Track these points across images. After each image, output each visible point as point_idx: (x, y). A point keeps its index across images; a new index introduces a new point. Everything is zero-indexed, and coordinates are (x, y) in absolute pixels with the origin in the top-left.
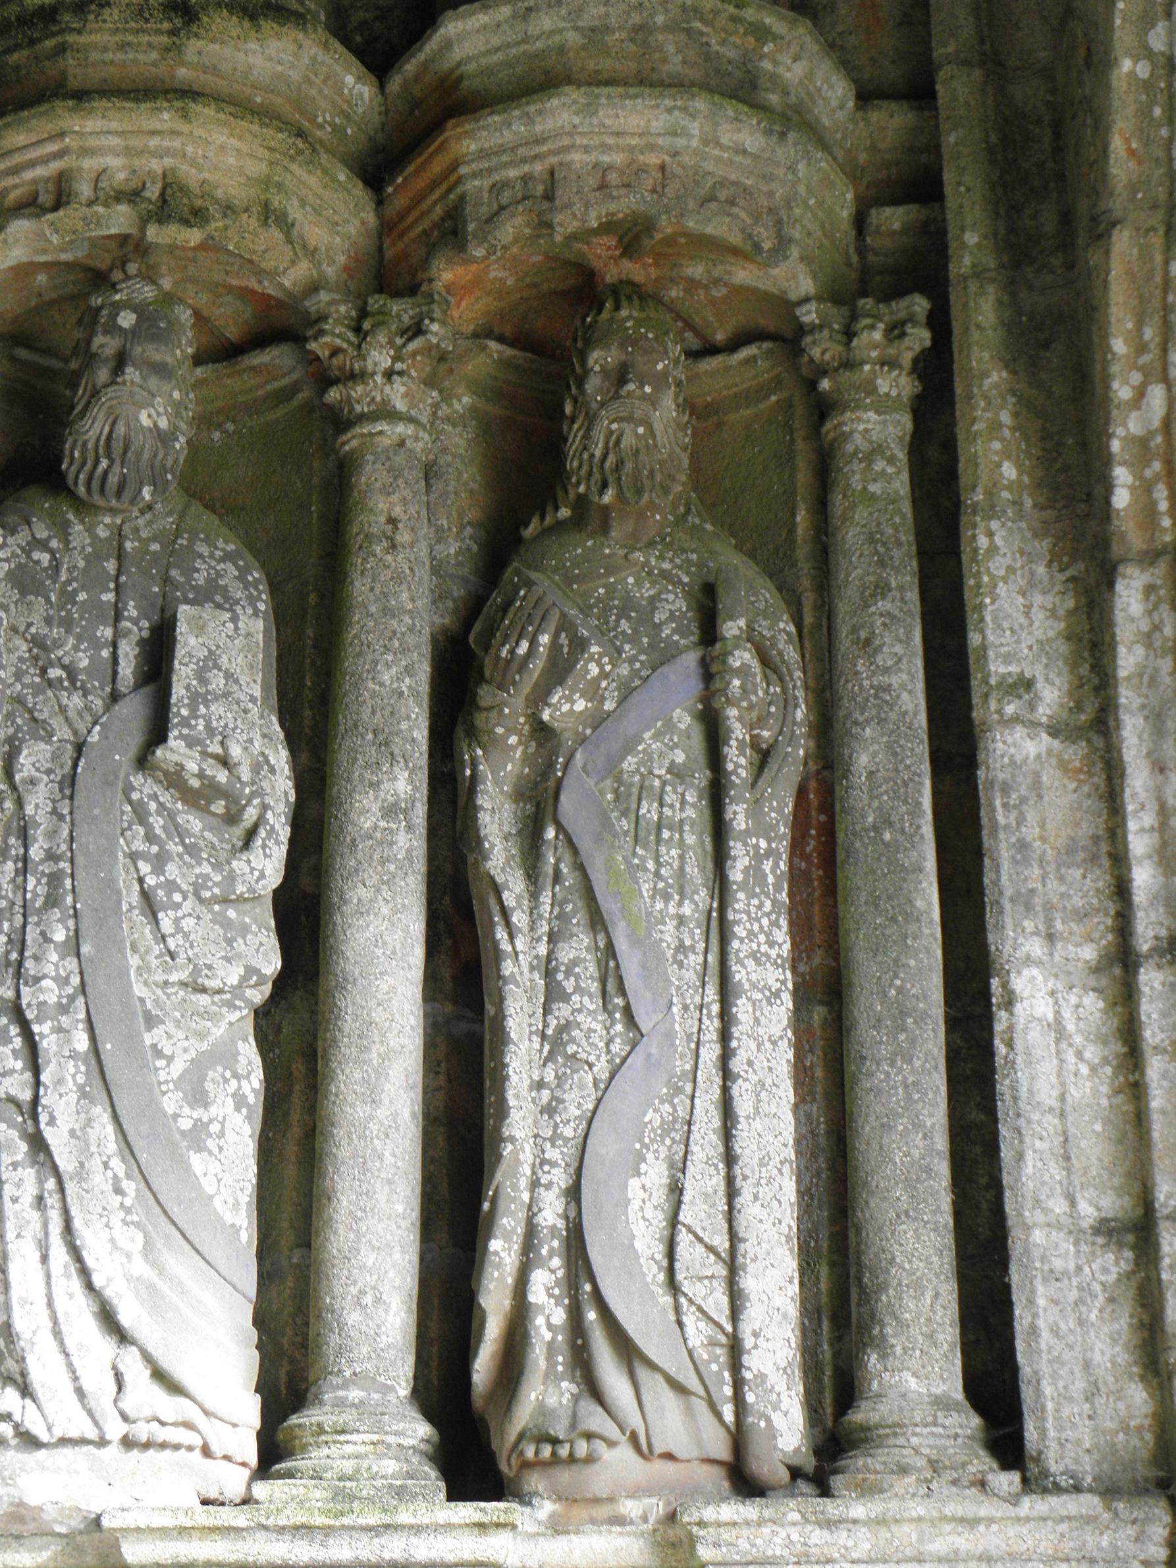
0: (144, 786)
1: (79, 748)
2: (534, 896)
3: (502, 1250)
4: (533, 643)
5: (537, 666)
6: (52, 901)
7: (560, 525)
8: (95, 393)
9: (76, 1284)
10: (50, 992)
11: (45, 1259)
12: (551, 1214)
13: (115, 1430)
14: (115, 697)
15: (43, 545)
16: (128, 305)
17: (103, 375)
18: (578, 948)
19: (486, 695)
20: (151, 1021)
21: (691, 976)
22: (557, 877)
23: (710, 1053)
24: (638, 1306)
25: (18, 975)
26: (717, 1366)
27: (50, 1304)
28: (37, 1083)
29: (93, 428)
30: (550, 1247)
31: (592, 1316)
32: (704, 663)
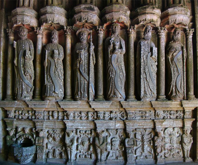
0: (151, 58)
1: (147, 56)
2: (172, 65)
3: (172, 86)
4: (173, 50)
5: (173, 51)
6: (146, 65)
7: (172, 42)
8: (147, 33)
9: (149, 88)
10: (147, 71)
11: (147, 87)
12: (174, 84)
13: (151, 97)
14: (149, 53)
15: (144, 43)
16: (149, 27)
17: (147, 32)
18: (175, 69)
19: (170, 53)
20: (152, 73)
21: (182, 71)
22: (174, 64)
23: (183, 75)
24: (179, 90)
25: (145, 70)
26: (183, 93)
27: (148, 89)
28: (146, 76)
29: (146, 35)
30: (174, 86)
31: (177, 90)
32: (182, 51)
